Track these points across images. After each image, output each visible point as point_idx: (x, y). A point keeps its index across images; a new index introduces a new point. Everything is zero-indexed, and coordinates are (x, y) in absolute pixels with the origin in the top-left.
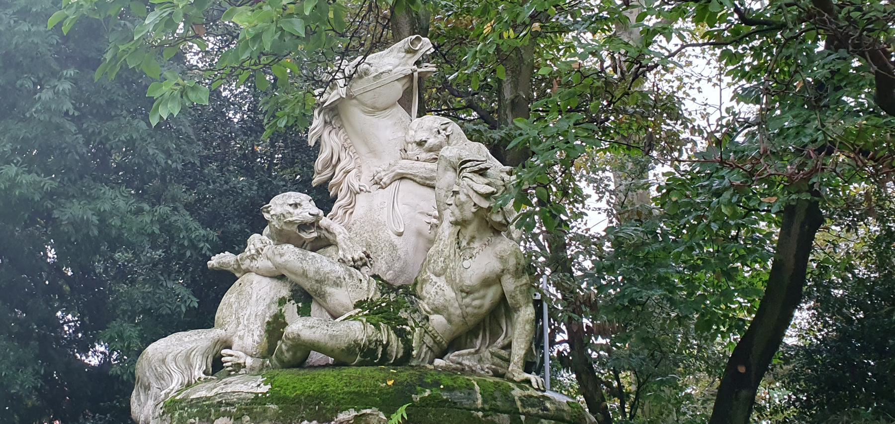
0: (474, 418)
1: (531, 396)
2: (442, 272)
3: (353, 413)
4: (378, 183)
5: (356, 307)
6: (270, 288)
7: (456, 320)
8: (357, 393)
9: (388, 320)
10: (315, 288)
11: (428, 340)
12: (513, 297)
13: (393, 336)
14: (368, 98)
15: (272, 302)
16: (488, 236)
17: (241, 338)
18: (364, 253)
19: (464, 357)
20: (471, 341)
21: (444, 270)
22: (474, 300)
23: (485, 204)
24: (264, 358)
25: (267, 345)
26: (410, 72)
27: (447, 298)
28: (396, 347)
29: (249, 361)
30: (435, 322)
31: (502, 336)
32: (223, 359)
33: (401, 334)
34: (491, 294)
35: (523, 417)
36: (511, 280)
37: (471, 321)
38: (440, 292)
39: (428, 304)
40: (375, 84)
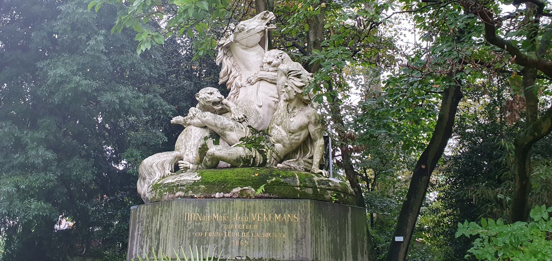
0: (296, 190)
1: (322, 180)
3: (240, 189)
4: (250, 82)
5: (240, 140)
7: (287, 145)
8: (242, 180)
9: (255, 147)
11: (274, 155)
12: (314, 135)
13: (258, 154)
14: (244, 42)
15: (201, 139)
16: (302, 106)
17: (187, 155)
18: (244, 115)
19: (291, 163)
20: (295, 156)
21: (281, 123)
22: (295, 136)
23: (300, 91)
24: (198, 164)
26: (264, 29)
27: (283, 136)
28: (259, 158)
29: (191, 166)
30: (277, 147)
31: (309, 153)
32: (179, 165)
33: (261, 152)
34: (304, 134)
35: (319, 190)
36: (313, 127)
37: (294, 147)
38: (280, 133)
39: (274, 139)
40: (247, 35)
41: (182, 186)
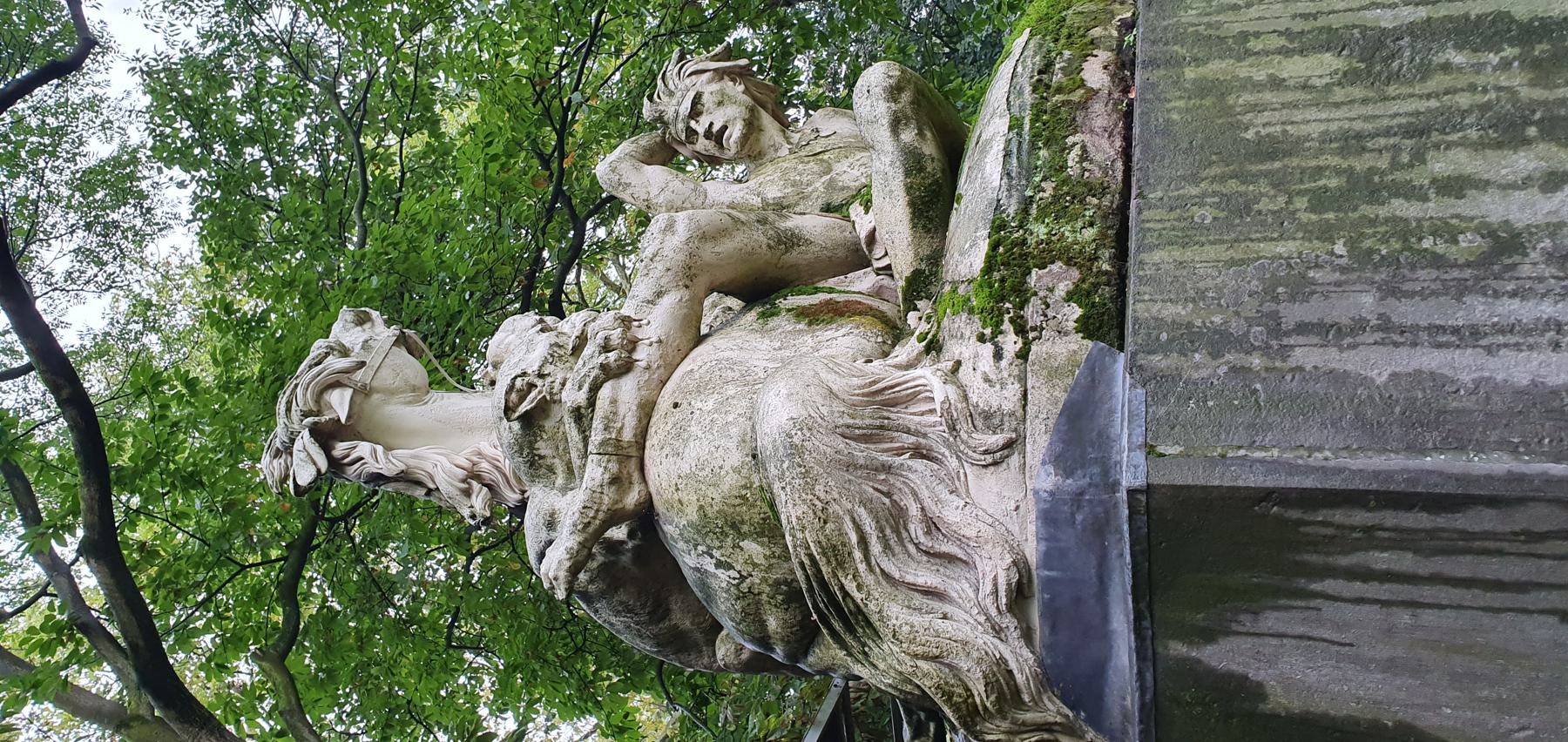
2: (825, 165)
10: (771, 232)
41: (1047, 68)
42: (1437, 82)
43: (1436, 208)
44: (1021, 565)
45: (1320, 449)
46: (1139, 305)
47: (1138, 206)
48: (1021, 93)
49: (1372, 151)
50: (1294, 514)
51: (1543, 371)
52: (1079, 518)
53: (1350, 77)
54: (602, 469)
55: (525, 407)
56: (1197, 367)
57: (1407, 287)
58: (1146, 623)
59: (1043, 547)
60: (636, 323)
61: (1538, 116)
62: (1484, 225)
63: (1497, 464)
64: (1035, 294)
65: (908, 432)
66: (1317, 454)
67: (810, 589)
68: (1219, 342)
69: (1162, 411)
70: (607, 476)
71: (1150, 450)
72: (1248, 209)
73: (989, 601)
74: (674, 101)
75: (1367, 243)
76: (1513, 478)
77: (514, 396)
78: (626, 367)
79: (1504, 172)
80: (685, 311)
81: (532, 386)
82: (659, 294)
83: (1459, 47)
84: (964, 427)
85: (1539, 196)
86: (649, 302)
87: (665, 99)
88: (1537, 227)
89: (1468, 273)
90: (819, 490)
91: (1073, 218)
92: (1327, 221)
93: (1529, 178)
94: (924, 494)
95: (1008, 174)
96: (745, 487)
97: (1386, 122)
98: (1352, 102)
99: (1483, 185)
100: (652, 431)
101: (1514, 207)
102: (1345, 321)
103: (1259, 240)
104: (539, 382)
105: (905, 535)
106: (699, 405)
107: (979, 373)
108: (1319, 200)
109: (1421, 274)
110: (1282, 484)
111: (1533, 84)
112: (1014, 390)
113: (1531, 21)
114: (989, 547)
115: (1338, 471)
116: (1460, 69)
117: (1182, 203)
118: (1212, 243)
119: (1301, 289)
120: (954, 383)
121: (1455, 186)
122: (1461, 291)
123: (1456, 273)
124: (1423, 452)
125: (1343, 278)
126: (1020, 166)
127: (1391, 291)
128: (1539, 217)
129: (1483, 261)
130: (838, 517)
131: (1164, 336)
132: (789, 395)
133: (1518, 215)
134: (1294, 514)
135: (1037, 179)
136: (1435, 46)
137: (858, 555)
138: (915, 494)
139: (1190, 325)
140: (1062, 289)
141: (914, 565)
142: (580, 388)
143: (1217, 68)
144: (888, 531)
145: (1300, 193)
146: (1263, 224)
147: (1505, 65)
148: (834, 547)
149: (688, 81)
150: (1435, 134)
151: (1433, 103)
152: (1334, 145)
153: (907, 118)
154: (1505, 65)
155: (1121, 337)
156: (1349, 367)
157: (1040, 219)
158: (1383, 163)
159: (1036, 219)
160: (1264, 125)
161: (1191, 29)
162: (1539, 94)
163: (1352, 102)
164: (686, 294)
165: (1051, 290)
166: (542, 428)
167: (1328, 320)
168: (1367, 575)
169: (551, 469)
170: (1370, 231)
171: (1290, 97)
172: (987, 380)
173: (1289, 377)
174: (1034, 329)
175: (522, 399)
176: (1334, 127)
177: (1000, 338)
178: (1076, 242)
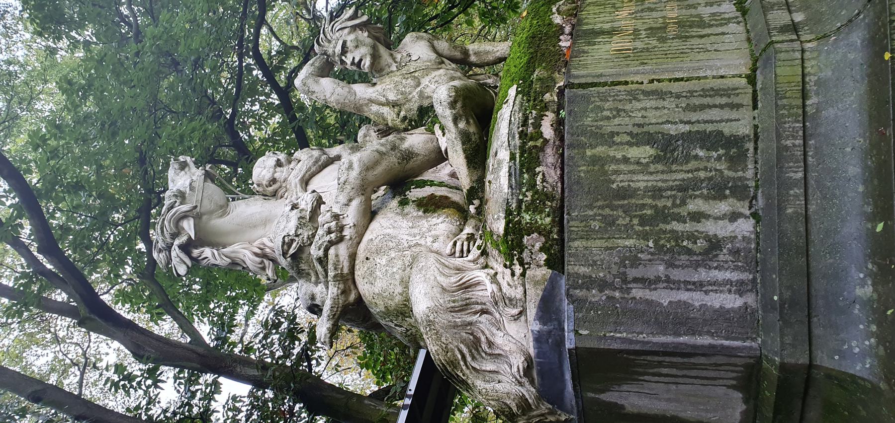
2: (417, 80)
6: (383, 218)
10: (399, 154)
25: (452, 209)
36: (440, 42)
38: (436, 78)
41: (525, 123)
42: (692, 165)
43: (688, 227)
44: (529, 360)
45: (642, 333)
46: (570, 267)
47: (567, 219)
48: (514, 137)
49: (665, 197)
50: (632, 357)
51: (724, 302)
52: (550, 341)
53: (657, 159)
54: (336, 289)
55: (292, 251)
56: (594, 296)
57: (677, 263)
58: (578, 388)
59: (536, 350)
60: (341, 217)
61: (730, 185)
62: (707, 236)
63: (705, 340)
64: (527, 248)
65: (478, 304)
66: (641, 336)
67: (443, 371)
68: (603, 285)
69: (581, 315)
70: (339, 291)
71: (576, 332)
72: (614, 222)
73: (516, 374)
74: (332, 46)
75: (662, 242)
76: (712, 346)
77: (285, 247)
78: (341, 239)
79: (716, 211)
80: (364, 207)
81: (292, 241)
82: (350, 200)
83: (702, 148)
84: (501, 304)
85: (728, 223)
86: (346, 205)
87: (327, 44)
88: (726, 238)
89: (700, 258)
90: (443, 339)
91: (541, 212)
92: (646, 230)
93: (725, 215)
94: (487, 332)
95: (511, 187)
96: (405, 301)
97: (671, 183)
98: (658, 172)
99: (707, 217)
100: (357, 267)
101: (719, 228)
102: (652, 277)
103: (618, 238)
104: (297, 239)
105: (480, 349)
106: (378, 261)
107: (505, 281)
108: (643, 221)
109: (682, 257)
110: (627, 348)
111: (729, 169)
112: (520, 289)
113: (731, 136)
114: (515, 354)
115: (648, 343)
116: (701, 159)
117: (585, 219)
118: (599, 239)
119: (635, 262)
120: (495, 283)
121: (697, 217)
122: (697, 266)
123: (695, 258)
124: (680, 335)
125: (652, 258)
126: (516, 183)
127: (670, 265)
128: (728, 233)
129: (706, 252)
130: (452, 349)
131: (580, 281)
132: (426, 294)
133: (720, 232)
134: (632, 357)
135: (524, 190)
136: (692, 146)
137: (462, 363)
138: (483, 332)
139: (591, 277)
140: (538, 245)
141: (485, 362)
142: (319, 249)
143: (600, 150)
144: (473, 351)
145: (635, 216)
146: (620, 230)
147: (719, 158)
148: (452, 362)
149: (337, 34)
150: (690, 190)
151: (690, 175)
152: (650, 194)
153: (461, 116)
154: (719, 158)
155: (563, 268)
156: (654, 298)
157: (527, 211)
158: (669, 204)
159: (525, 211)
160: (621, 181)
161: (589, 129)
162: (731, 174)
163: (658, 172)
164: (363, 198)
165: (533, 246)
166: (301, 258)
167: (646, 277)
168: (660, 375)
169: (308, 274)
170: (663, 236)
171: (632, 167)
172: (509, 285)
173: (630, 302)
174: (527, 264)
175: (290, 246)
176: (650, 184)
177: (513, 267)
178: (542, 224)
